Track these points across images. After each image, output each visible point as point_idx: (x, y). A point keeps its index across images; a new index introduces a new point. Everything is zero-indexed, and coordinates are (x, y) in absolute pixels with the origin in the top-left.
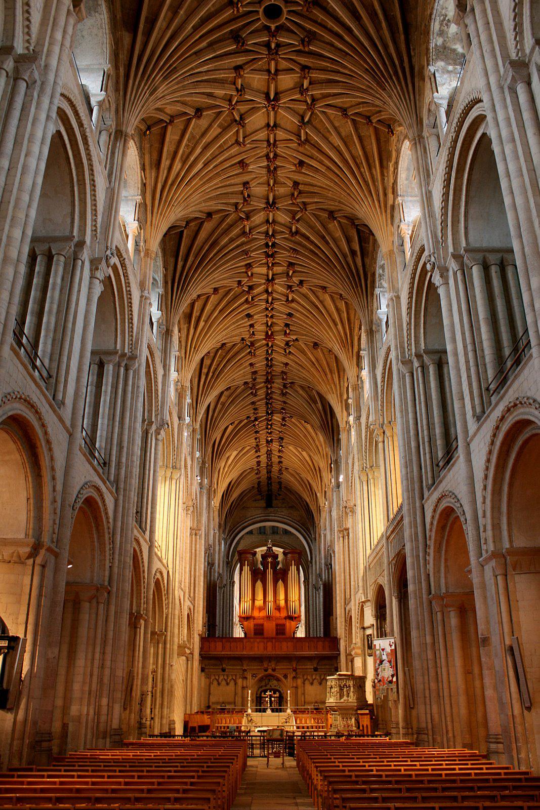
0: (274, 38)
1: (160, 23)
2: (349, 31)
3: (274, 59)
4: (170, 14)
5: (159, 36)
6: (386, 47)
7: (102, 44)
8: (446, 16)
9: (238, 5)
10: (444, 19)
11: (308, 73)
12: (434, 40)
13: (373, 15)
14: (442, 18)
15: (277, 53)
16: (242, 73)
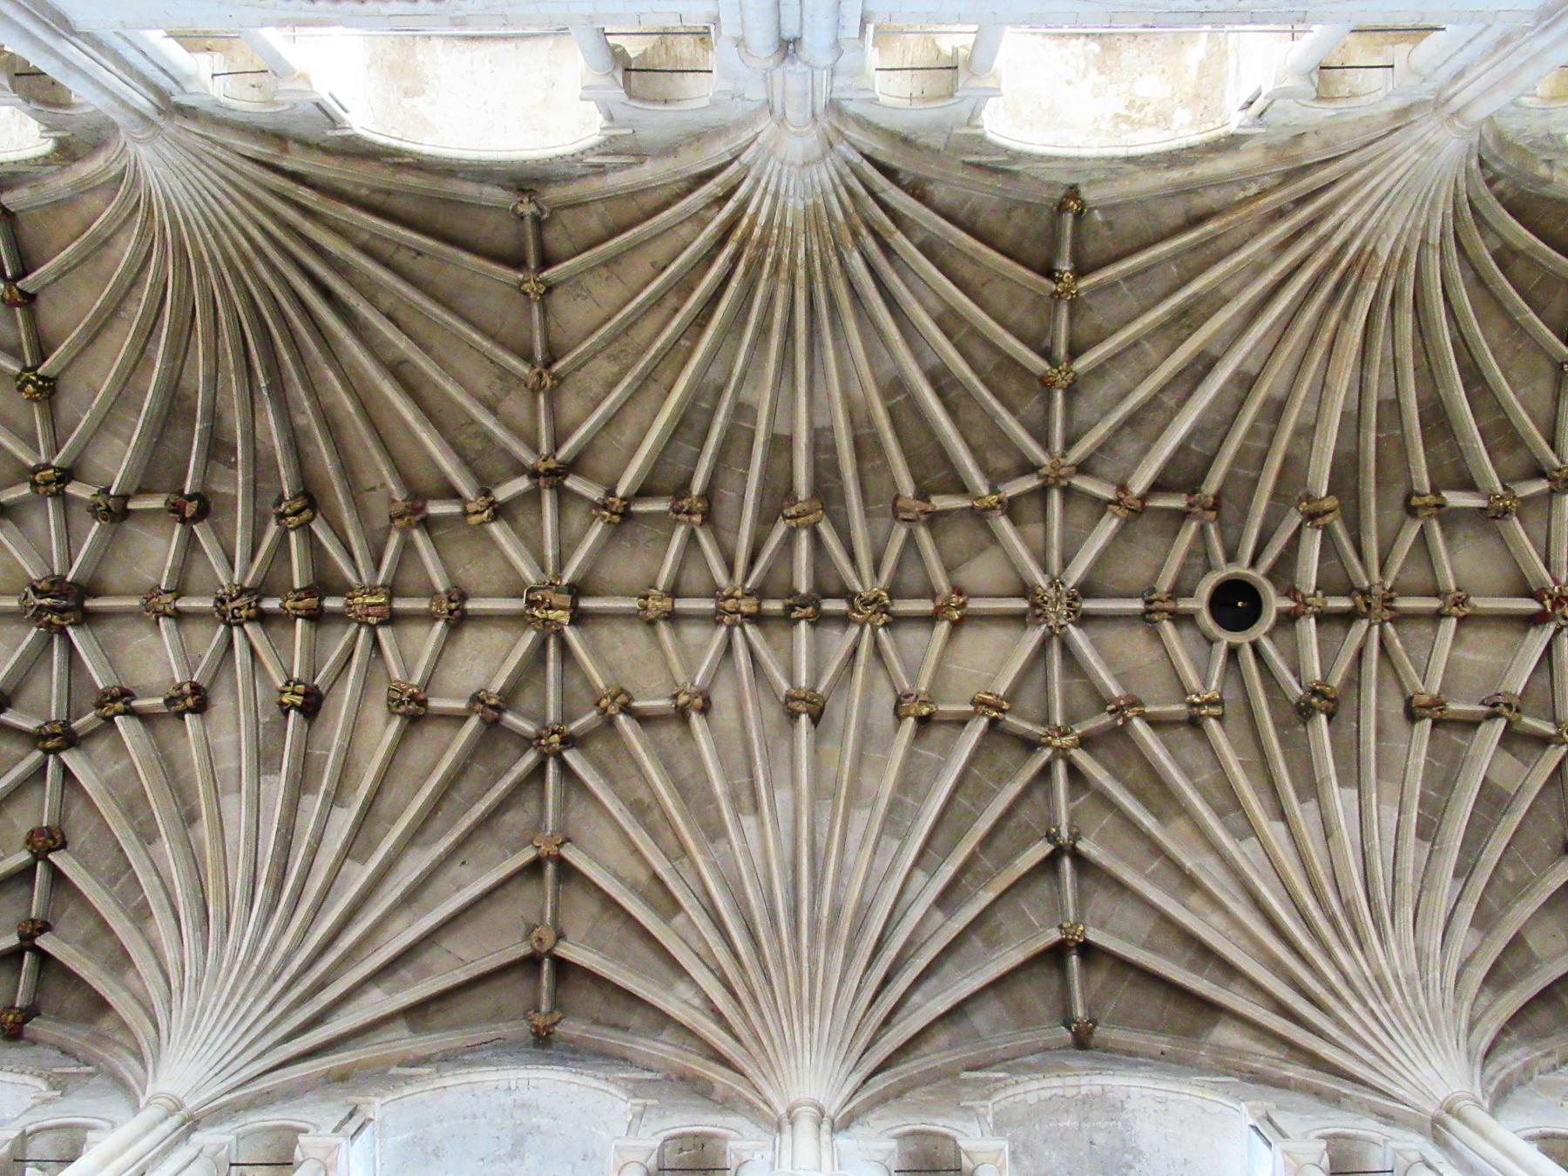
0: (1309, 600)
1: (1209, 930)
2: (1246, 382)
3: (1387, 601)
4: (1195, 900)
5: (1243, 942)
6: (1259, 269)
7: (1204, 1111)
8: (1117, 116)
9: (1193, 704)
10: (1127, 119)
11: (1420, 495)
12: (1181, 133)
13: (1187, 319)
14: (1124, 127)
15: (1365, 593)
16: (1425, 699)
